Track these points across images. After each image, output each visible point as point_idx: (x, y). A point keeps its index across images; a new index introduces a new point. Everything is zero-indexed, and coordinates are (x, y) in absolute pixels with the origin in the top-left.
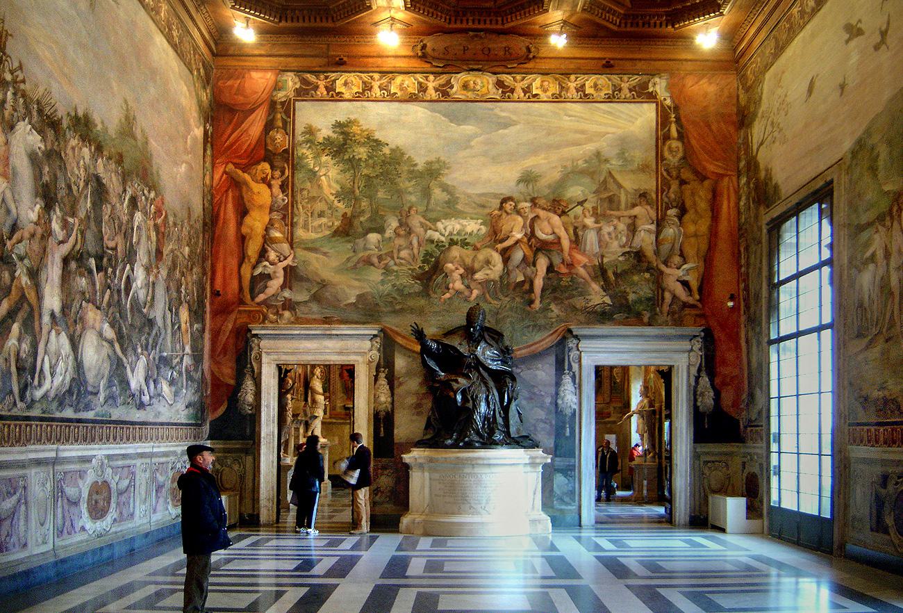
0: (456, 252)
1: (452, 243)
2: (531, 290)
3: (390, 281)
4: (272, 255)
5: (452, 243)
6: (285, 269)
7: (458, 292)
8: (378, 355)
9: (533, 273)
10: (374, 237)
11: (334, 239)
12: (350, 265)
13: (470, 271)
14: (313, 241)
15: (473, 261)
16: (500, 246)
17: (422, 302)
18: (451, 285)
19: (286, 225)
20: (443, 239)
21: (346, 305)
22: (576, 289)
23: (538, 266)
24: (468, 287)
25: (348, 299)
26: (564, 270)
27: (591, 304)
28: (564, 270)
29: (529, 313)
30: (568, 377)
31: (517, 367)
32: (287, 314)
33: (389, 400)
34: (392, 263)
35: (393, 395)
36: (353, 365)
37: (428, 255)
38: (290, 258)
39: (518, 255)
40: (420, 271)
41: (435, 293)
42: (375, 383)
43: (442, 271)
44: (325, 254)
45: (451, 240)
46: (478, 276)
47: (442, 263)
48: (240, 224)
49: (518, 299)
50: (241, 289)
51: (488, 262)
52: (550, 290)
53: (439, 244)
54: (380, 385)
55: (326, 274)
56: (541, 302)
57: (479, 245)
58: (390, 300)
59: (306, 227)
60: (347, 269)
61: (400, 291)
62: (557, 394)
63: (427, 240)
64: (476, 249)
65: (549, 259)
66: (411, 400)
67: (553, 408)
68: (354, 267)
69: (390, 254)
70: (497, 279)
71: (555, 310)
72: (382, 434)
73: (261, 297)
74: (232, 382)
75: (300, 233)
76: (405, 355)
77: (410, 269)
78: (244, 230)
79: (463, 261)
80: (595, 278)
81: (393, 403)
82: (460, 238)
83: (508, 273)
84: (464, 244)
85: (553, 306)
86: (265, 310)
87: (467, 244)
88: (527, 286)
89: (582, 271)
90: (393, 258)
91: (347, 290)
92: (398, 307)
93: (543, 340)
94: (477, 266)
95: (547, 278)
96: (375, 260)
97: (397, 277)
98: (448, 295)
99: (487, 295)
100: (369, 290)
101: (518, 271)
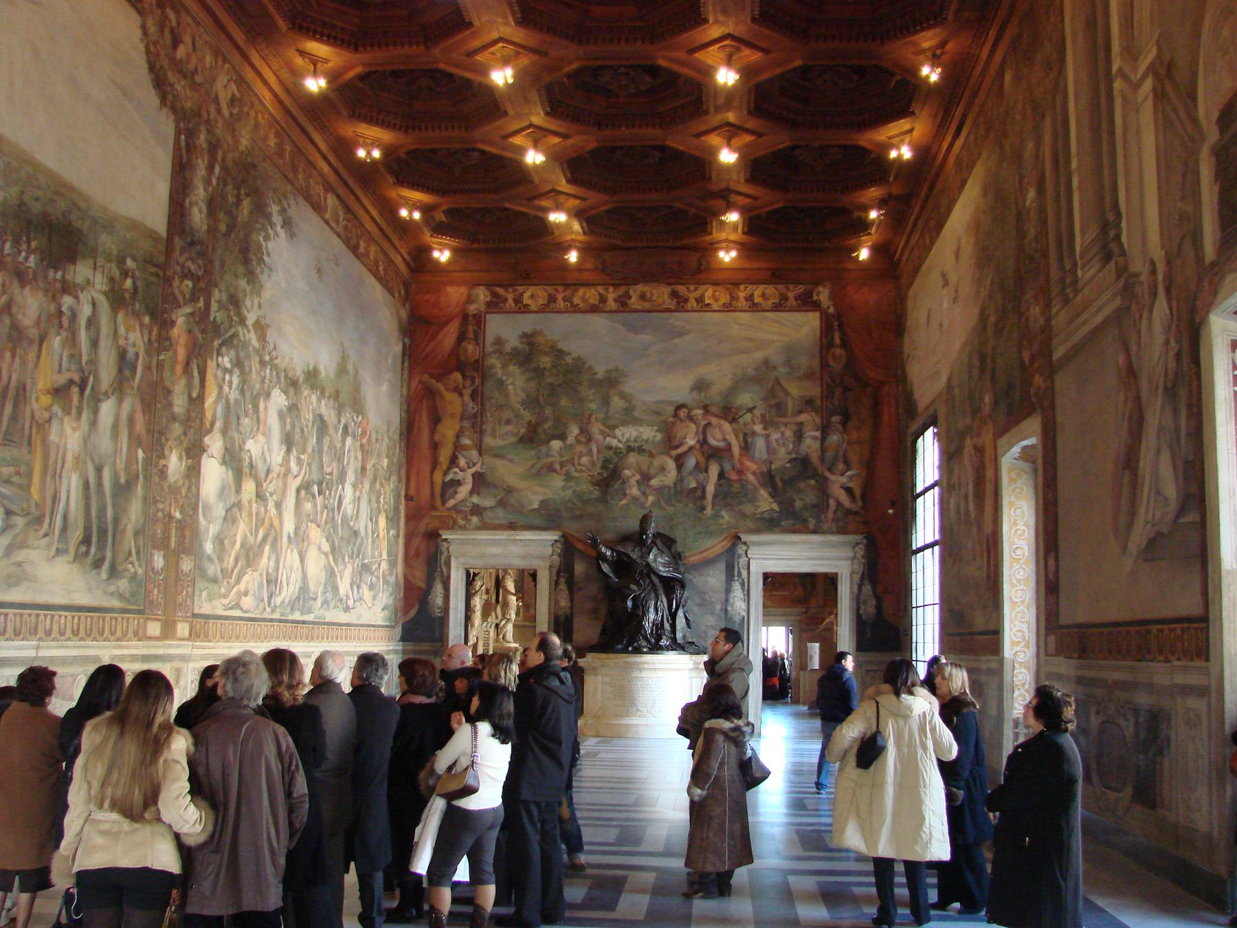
0: (633, 458)
1: (630, 449)
2: (703, 497)
4: (462, 462)
5: (630, 449)
6: (473, 475)
7: (635, 499)
8: (559, 559)
10: (556, 444)
12: (534, 471)
13: (646, 478)
14: (501, 448)
15: (649, 467)
16: (674, 453)
17: (601, 508)
18: (628, 491)
19: (476, 432)
20: (620, 445)
22: (746, 494)
24: (644, 493)
26: (734, 477)
27: (760, 510)
28: (734, 477)
30: (737, 584)
32: (475, 519)
33: (569, 604)
34: (573, 469)
35: (572, 601)
37: (607, 461)
38: (479, 464)
39: (691, 462)
40: (600, 478)
43: (619, 477)
44: (511, 461)
45: (629, 447)
46: (654, 482)
48: (433, 431)
49: (691, 506)
50: (433, 495)
51: (663, 469)
53: (616, 451)
55: (513, 481)
57: (654, 452)
58: (570, 505)
59: (494, 435)
61: (579, 496)
62: (727, 600)
64: (652, 455)
65: (721, 465)
66: (589, 605)
67: (723, 614)
68: (538, 473)
69: (572, 461)
70: (672, 485)
71: (726, 517)
73: (451, 503)
74: (423, 585)
75: (489, 441)
78: (437, 437)
79: (640, 468)
80: (764, 485)
81: (572, 608)
82: (636, 445)
84: (641, 450)
85: (723, 513)
86: (454, 515)
87: (644, 451)
88: (699, 493)
89: (751, 478)
90: (573, 464)
92: (578, 513)
94: (652, 472)
95: (718, 485)
96: (557, 467)
97: (578, 483)
98: (624, 502)
99: (662, 502)
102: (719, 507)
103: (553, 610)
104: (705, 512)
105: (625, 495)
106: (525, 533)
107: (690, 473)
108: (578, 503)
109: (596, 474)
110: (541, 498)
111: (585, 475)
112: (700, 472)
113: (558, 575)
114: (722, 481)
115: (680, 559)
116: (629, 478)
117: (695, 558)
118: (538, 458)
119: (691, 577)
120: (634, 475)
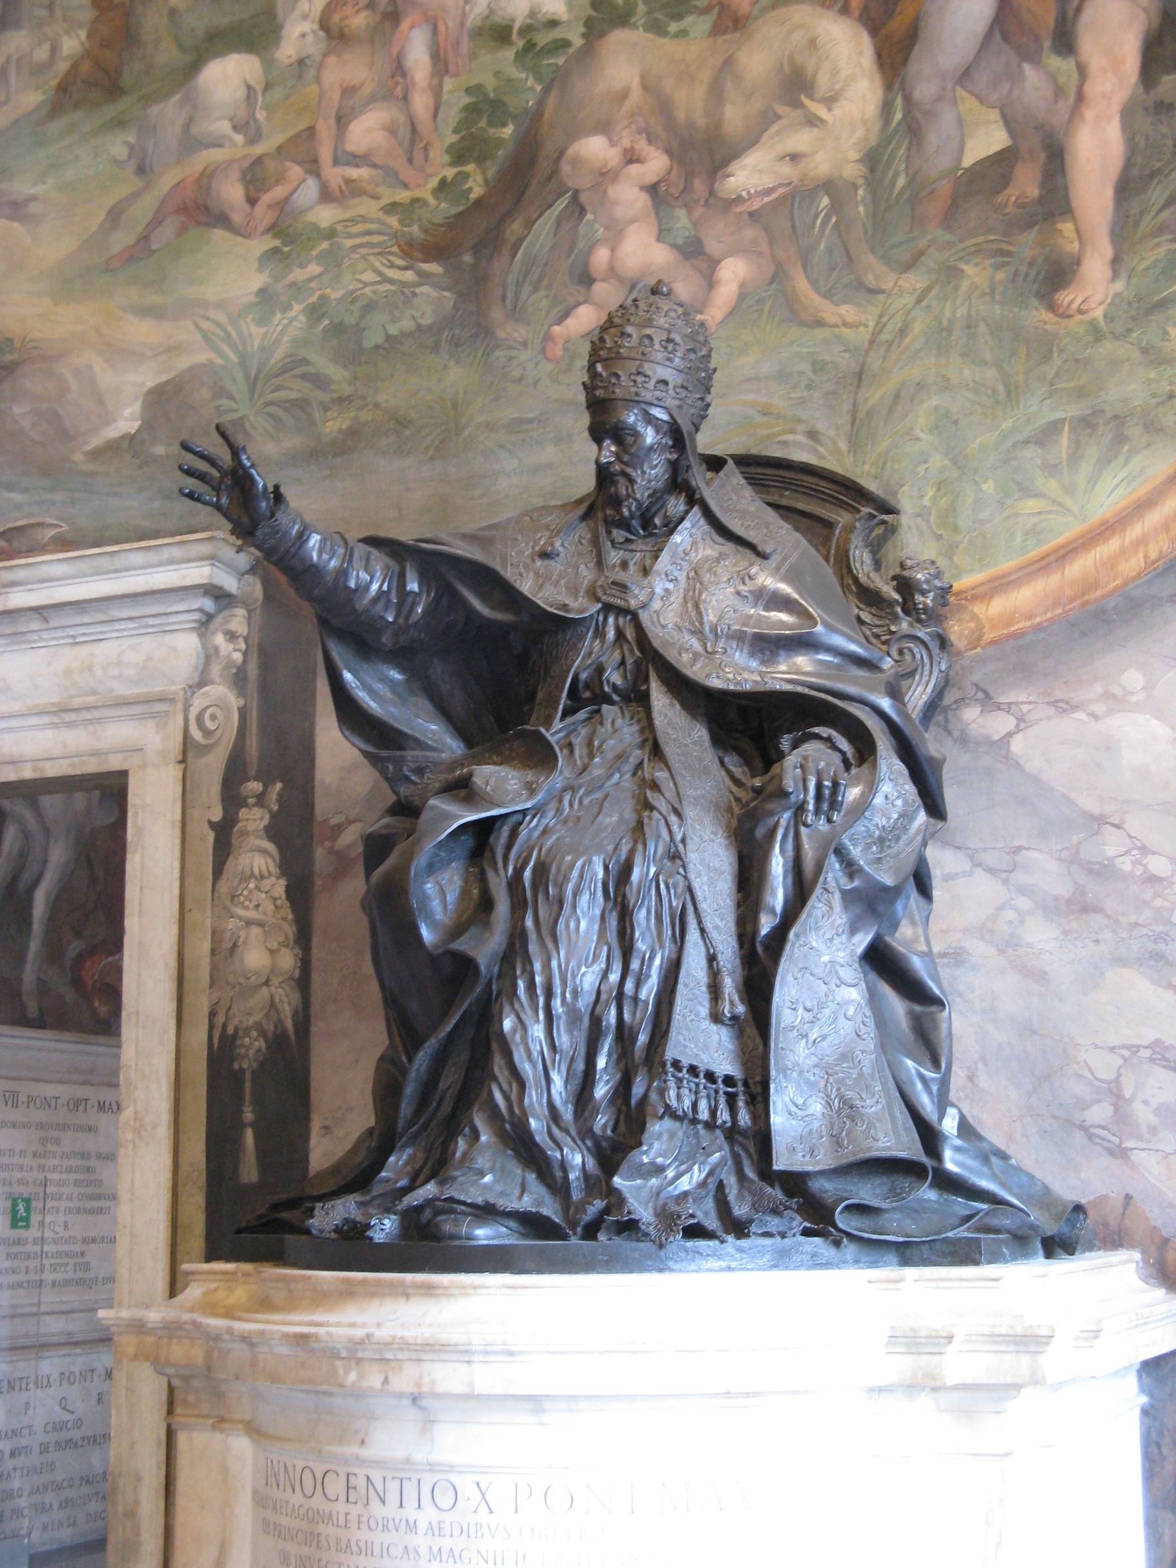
3: (297, 288)
8: (234, 702)
9: (1059, 91)
11: (54, 127)
12: (121, 240)
15: (716, 93)
18: (601, 256)
21: (97, 454)
23: (1089, 46)
25: (108, 418)
29: (1045, 347)
31: (988, 702)
33: (288, 960)
34: (309, 190)
35: (304, 936)
36: (124, 774)
40: (446, 209)
41: (516, 313)
42: (218, 872)
49: (975, 273)
54: (247, 877)
56: (1116, 262)
58: (295, 389)
60: (109, 268)
63: (477, 33)
70: (853, 171)
72: (249, 1172)
79: (664, 107)
81: (303, 981)
83: (914, 130)
90: (313, 166)
91: (107, 378)
92: (333, 425)
93: (1141, 507)
94: (734, 116)
96: (232, 193)
97: (333, 261)
99: (802, 285)
100: (203, 356)
101: (968, 104)
103: (200, 1003)
104: (1065, 297)
105: (586, 279)
106: (52, 564)
107: (965, 76)
108: (337, 373)
110: (148, 377)
113: (232, 799)
116: (607, 176)
117: (1024, 596)
118: (141, 170)
119: (998, 725)
120: (631, 158)
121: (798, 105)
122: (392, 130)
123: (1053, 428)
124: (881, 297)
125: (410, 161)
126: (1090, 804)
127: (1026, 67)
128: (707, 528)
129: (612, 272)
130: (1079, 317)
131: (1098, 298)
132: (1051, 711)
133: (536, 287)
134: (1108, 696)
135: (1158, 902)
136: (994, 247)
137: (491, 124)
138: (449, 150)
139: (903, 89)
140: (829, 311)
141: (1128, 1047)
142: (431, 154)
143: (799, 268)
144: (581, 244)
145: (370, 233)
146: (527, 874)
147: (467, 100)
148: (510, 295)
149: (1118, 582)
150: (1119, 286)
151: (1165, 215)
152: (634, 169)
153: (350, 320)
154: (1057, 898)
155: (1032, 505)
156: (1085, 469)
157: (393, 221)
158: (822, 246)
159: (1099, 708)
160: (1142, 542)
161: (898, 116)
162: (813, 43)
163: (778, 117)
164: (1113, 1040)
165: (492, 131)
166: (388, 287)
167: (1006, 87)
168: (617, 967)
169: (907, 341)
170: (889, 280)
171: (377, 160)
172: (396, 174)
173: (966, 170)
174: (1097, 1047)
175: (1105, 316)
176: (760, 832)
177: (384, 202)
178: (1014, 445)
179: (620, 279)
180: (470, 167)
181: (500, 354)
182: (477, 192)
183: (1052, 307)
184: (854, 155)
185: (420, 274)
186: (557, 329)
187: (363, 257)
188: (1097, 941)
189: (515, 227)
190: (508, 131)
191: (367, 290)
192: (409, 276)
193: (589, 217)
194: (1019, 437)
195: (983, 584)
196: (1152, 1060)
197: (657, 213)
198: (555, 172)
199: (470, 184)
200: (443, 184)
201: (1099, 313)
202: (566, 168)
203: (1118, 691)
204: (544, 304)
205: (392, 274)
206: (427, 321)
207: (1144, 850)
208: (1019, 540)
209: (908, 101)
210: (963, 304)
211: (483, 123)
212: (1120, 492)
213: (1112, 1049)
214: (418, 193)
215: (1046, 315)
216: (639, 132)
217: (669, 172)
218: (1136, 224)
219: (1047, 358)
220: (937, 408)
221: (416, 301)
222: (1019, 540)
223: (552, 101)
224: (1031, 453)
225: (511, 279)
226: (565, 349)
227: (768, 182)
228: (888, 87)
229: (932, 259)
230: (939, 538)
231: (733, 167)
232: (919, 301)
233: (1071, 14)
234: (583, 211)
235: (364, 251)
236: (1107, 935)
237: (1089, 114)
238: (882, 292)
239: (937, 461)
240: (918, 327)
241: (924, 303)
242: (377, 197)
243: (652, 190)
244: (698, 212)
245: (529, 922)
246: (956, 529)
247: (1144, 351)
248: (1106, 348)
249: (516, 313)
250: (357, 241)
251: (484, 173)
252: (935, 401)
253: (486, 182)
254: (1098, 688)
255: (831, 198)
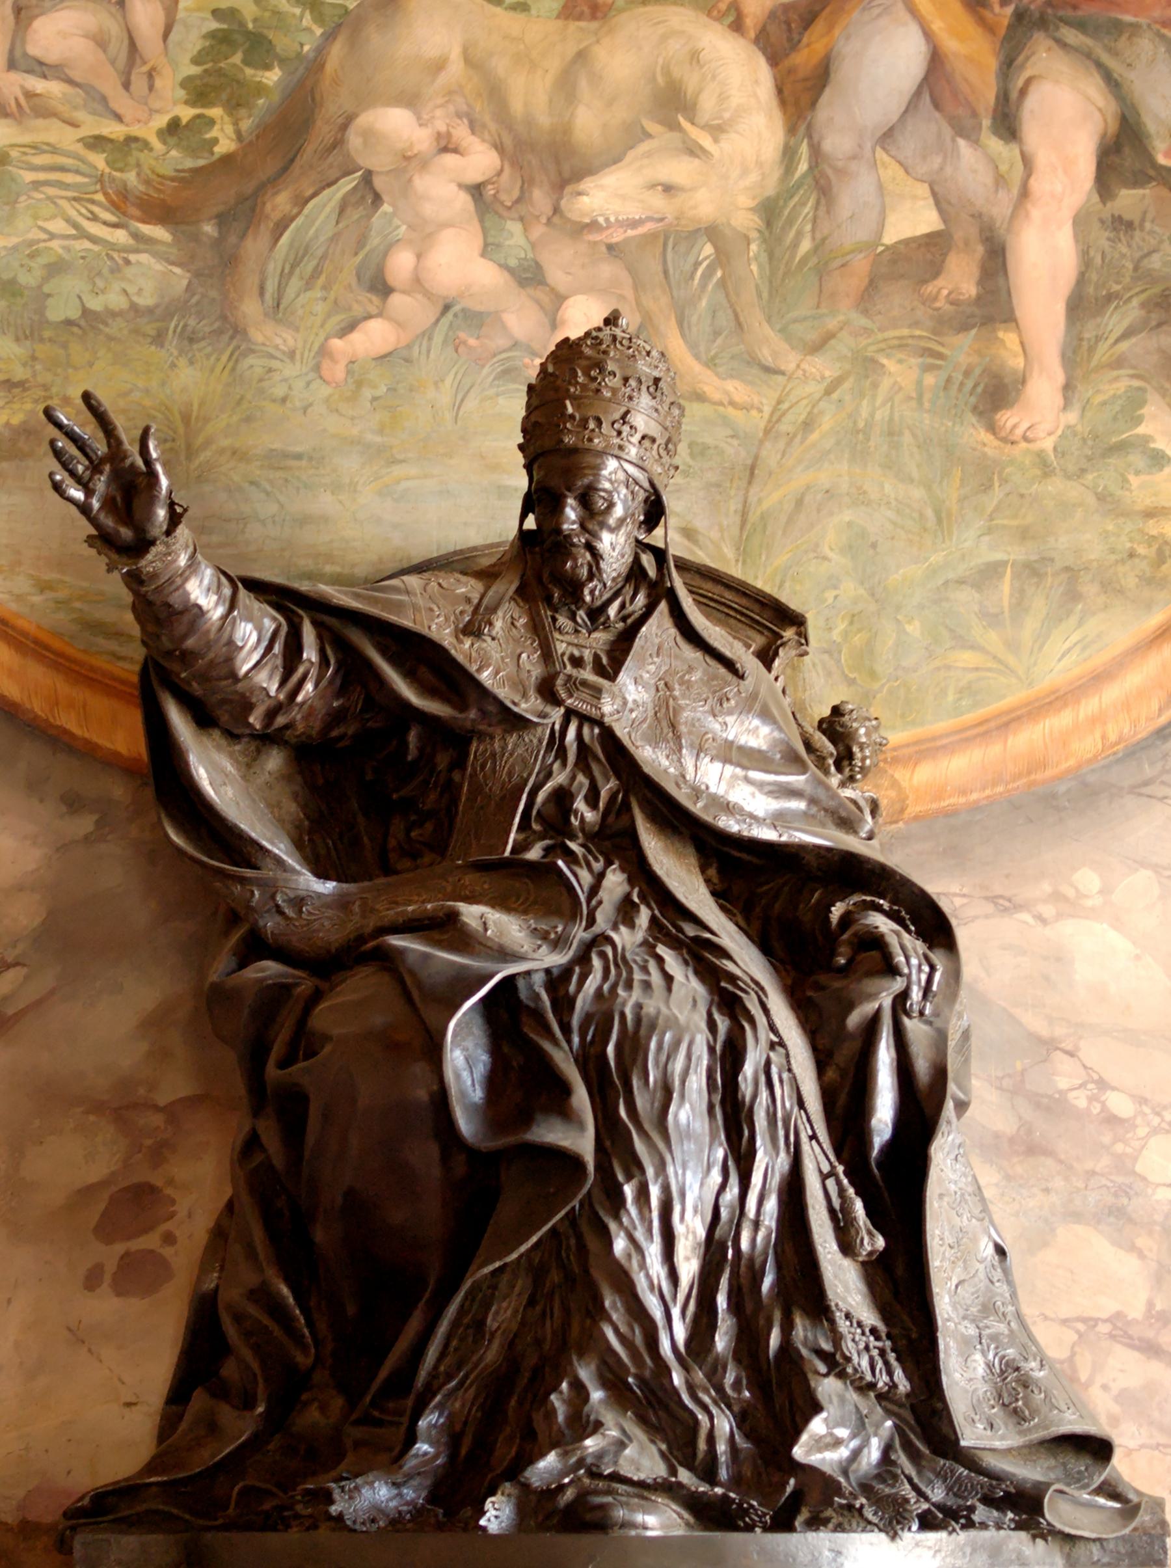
9: (1000, 180)
18: (401, 263)
41: (277, 310)
47: (331, 109)
52: (1132, 312)
65: (1112, 83)
70: (745, 220)
76: (34, 786)
77: (97, 142)
79: (495, 93)
93: (1098, 678)
101: (891, 171)
102: (1120, 384)
104: (1008, 418)
105: (382, 288)
107: (887, 137)
109: (149, 130)
111: (67, 138)
112: (965, 130)
114: (1128, 199)
115: (845, 758)
120: (446, 146)
121: (674, 126)
122: (101, 41)
123: (992, 571)
124: (780, 379)
125: (127, 85)
126: (1035, 1023)
127: (961, 142)
128: (673, 631)
129: (418, 283)
130: (1024, 445)
131: (1047, 426)
132: (989, 908)
133: (309, 284)
134: (1057, 897)
135: (1119, 1148)
136: (923, 344)
137: (247, 62)
138: (186, 83)
139: (810, 137)
140: (712, 384)
141: (1084, 1320)
142: (158, 83)
143: (673, 321)
144: (374, 241)
145: (63, 169)
146: (610, 1049)
147: (214, 25)
148: (271, 287)
149: (1072, 762)
150: (1072, 417)
151: (1124, 346)
152: (449, 159)
153: (24, 279)
154: (997, 1136)
155: (967, 658)
156: (1031, 625)
157: (99, 160)
158: (704, 303)
159: (1048, 911)
160: (1097, 720)
161: (803, 167)
162: (695, 57)
163: (648, 136)
164: (1065, 1312)
165: (249, 71)
166: (87, 244)
167: (937, 161)
168: (734, 1180)
169: (814, 436)
170: (790, 361)
171: (76, 75)
172: (104, 100)
173: (887, 248)
174: (1046, 1318)
175: (1055, 449)
176: (854, 1019)
177: (85, 131)
178: (946, 583)
179: (428, 294)
180: (216, 112)
181: (253, 364)
182: (226, 145)
183: (992, 428)
184: (745, 201)
185: (136, 236)
186: (336, 343)
187: (51, 199)
188: (1047, 1190)
189: (280, 202)
190: (272, 77)
191: (55, 244)
192: (120, 236)
193: (386, 208)
194: (951, 575)
195: (908, 745)
196: (1112, 1336)
197: (482, 221)
198: (338, 143)
199: (214, 133)
200: (174, 126)
201: (1048, 444)
202: (354, 141)
203: (1071, 893)
204: (320, 308)
205: (95, 229)
206: (146, 300)
207: (1103, 1085)
208: (951, 698)
209: (816, 152)
210: (884, 404)
211: (237, 58)
212: (1073, 657)
213: (1065, 1322)
214: (136, 131)
215: (984, 436)
216: (459, 115)
217: (500, 173)
218: (1091, 350)
219: (987, 487)
220: (850, 524)
221: (129, 271)
222: (951, 698)
223: (337, 50)
224: (965, 597)
225: (273, 269)
226: (349, 372)
227: (633, 211)
228: (791, 130)
229: (844, 344)
230: (851, 682)
231: (587, 184)
232: (828, 392)
233: (1014, 95)
234: (377, 199)
235: (52, 191)
236: (1058, 1183)
237: (1036, 213)
238: (783, 373)
239: (850, 589)
240: (827, 423)
241: (835, 396)
242: (74, 125)
243: (476, 191)
244: (538, 231)
245: (623, 1112)
246: (873, 675)
247: (1101, 498)
248: (1055, 486)
249: (277, 310)
250: (42, 176)
251: (236, 123)
252: (847, 516)
253: (239, 136)
254: (1047, 887)
255: (716, 247)
